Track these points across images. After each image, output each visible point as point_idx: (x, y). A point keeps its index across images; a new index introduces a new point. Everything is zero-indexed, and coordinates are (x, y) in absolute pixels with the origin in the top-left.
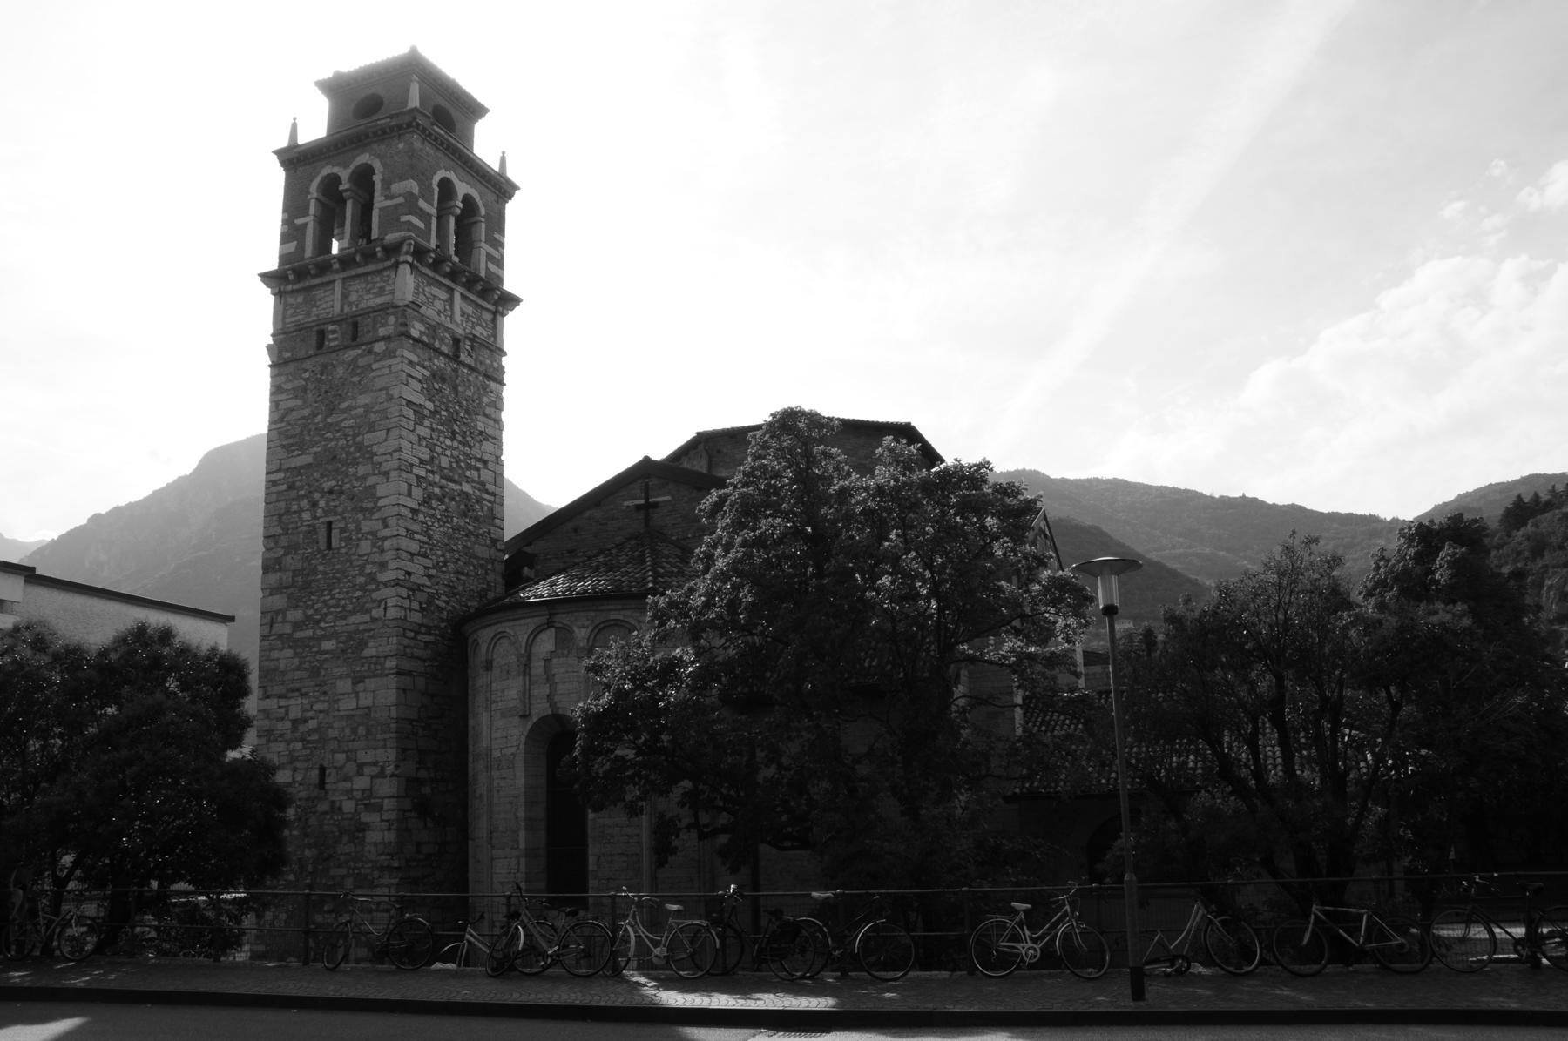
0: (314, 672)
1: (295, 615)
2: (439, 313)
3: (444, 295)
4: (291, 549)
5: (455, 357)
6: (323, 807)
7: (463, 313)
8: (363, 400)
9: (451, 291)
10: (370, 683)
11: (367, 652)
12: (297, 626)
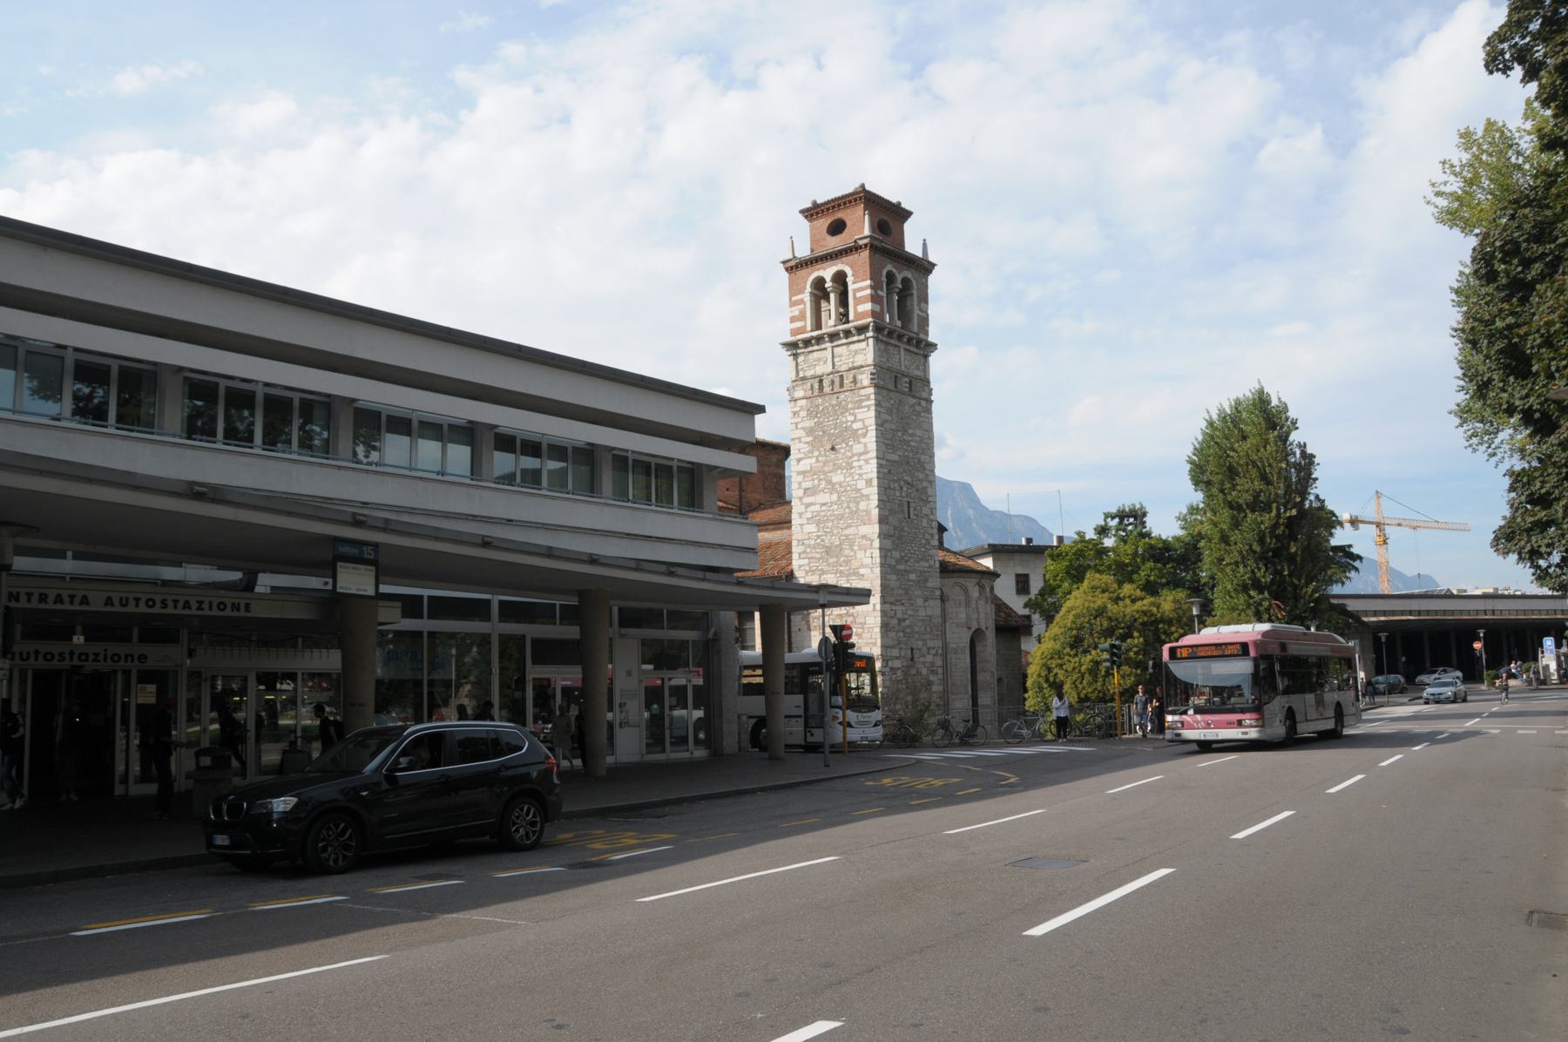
0: (907, 591)
1: (896, 554)
4: (892, 512)
6: (913, 671)
8: (919, 433)
10: (931, 602)
11: (929, 584)
12: (898, 562)
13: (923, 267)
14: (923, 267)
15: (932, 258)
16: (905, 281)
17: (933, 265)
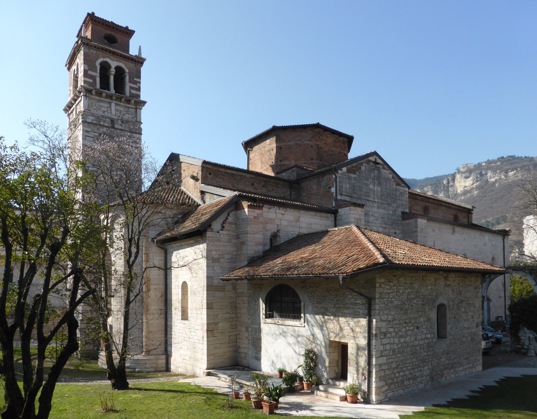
2: (104, 112)
3: (106, 105)
5: (113, 127)
7: (117, 110)
9: (110, 103)
13: (139, 61)
14: (139, 61)
15: (143, 56)
16: (118, 68)
17: (144, 60)
